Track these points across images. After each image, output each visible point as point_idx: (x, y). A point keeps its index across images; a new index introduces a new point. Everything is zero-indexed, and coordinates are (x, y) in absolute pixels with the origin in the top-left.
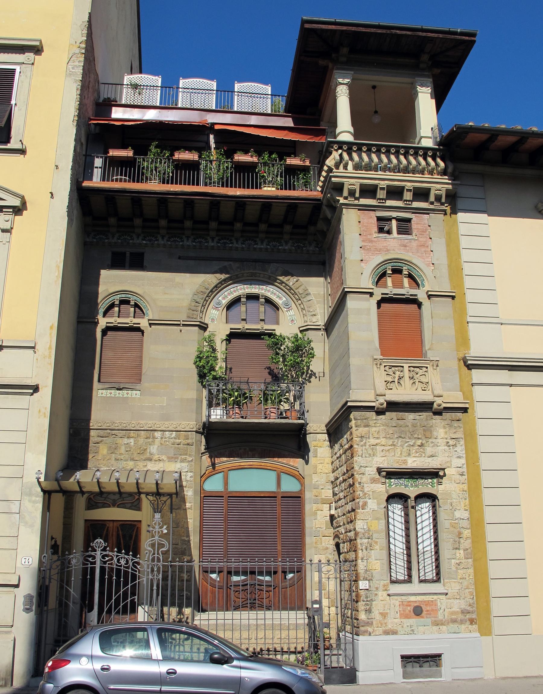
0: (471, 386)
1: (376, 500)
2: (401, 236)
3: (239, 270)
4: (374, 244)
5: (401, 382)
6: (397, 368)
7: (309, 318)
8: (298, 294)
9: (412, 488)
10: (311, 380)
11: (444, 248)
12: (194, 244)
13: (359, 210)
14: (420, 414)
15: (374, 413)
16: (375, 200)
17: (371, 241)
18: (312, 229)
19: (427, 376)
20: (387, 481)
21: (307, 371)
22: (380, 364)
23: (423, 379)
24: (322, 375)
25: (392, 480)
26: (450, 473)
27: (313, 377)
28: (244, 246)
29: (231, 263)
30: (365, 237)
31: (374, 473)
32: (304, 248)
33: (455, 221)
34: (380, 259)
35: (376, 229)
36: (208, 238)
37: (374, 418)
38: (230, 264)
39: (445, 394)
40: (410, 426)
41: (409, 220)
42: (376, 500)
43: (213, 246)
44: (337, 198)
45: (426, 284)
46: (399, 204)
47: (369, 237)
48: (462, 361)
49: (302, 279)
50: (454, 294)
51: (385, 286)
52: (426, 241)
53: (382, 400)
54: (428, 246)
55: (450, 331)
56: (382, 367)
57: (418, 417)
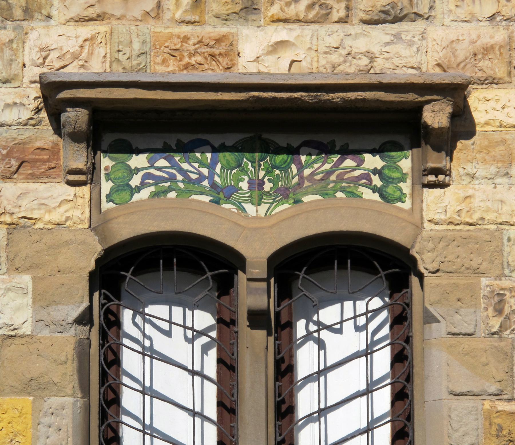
1: (26, 280)
9: (256, 210)
20: (106, 162)
25: (138, 161)
26: (500, 116)
31: (26, 115)
42: (26, 280)
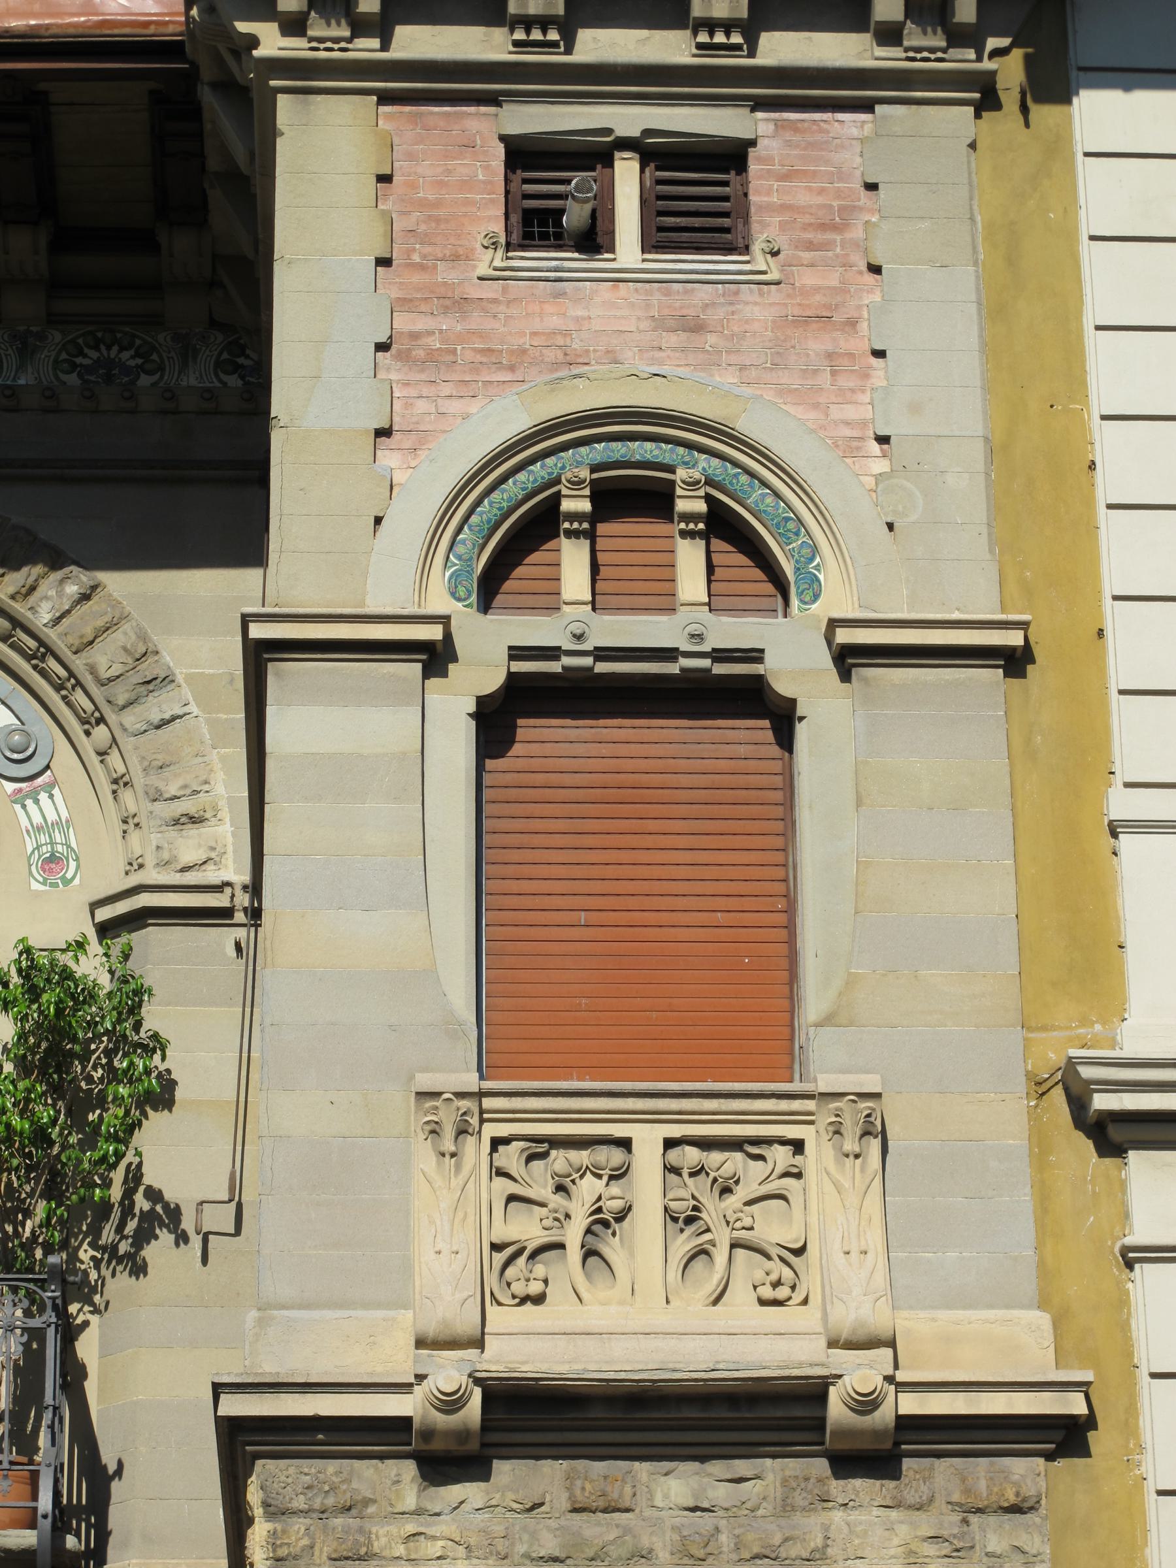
0: (1117, 1269)
2: (666, 262)
4: (476, 321)
5: (612, 1248)
6: (582, 1157)
7: (155, 839)
8: (88, 680)
10: (150, 1252)
11: (962, 329)
13: (385, 98)
14: (742, 1467)
15: (409, 1469)
16: (499, 35)
17: (460, 304)
19: (796, 1200)
21: (129, 1194)
22: (462, 1131)
23: (773, 1228)
24: (223, 1219)
27: (165, 1237)
30: (417, 278)
32: (145, 380)
33: (1059, 147)
34: (506, 418)
35: (492, 219)
37: (410, 1500)
39: (912, 1325)
40: (663, 1555)
41: (732, 156)
44: (243, 27)
45: (830, 575)
46: (670, 47)
47: (446, 274)
48: (1058, 1095)
49: (122, 585)
50: (1015, 639)
51: (548, 600)
52: (843, 289)
53: (449, 1372)
54: (852, 323)
55: (983, 893)
56: (475, 1151)
57: (721, 1493)
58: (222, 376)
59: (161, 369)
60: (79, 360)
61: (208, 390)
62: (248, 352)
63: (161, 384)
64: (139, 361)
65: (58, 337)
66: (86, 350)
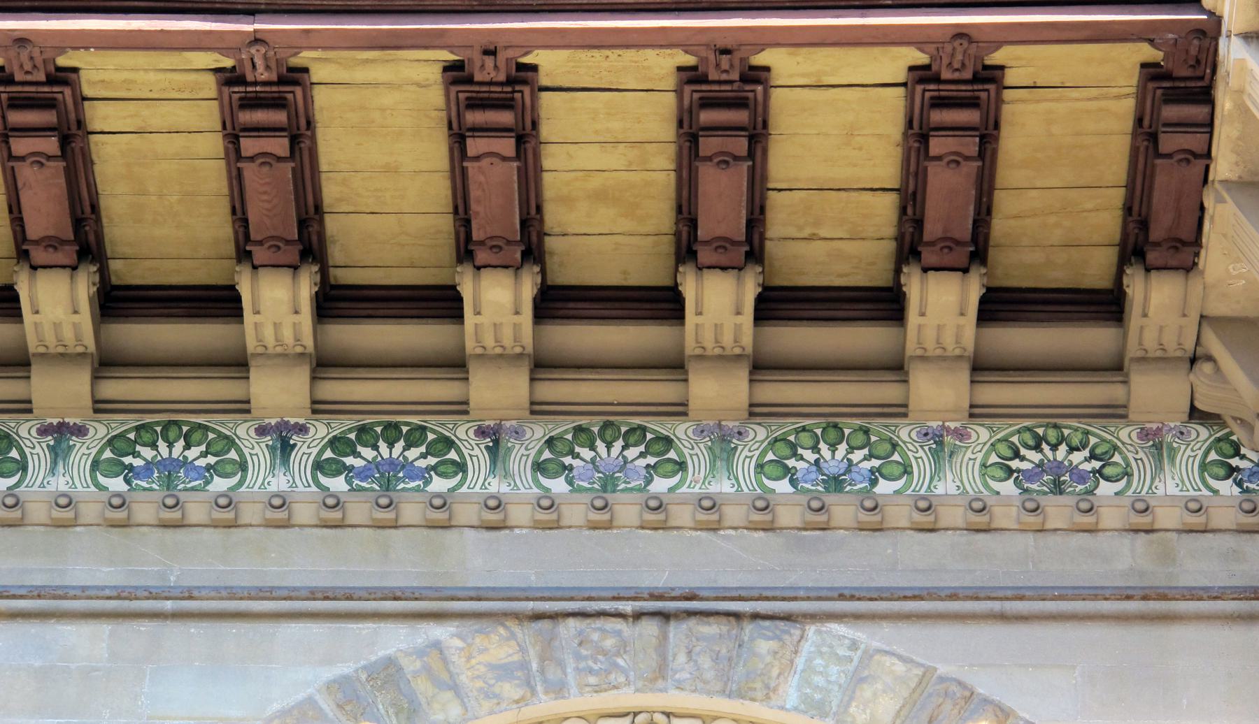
3: (510, 690)
12: (117, 484)
18: (1156, 300)
28: (558, 485)
29: (440, 632)
36: (244, 431)
38: (437, 646)
43: (281, 503)
58: (1212, 482)
59: (1127, 474)
60: (1015, 464)
61: (1194, 500)
62: (1243, 451)
63: (1130, 493)
64: (1097, 464)
65: (984, 434)
66: (1023, 451)
